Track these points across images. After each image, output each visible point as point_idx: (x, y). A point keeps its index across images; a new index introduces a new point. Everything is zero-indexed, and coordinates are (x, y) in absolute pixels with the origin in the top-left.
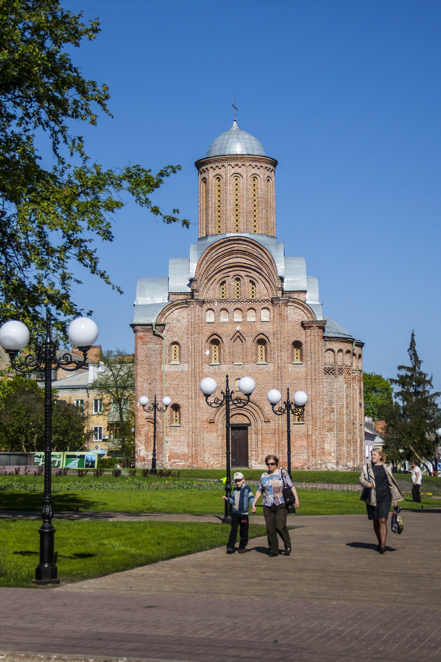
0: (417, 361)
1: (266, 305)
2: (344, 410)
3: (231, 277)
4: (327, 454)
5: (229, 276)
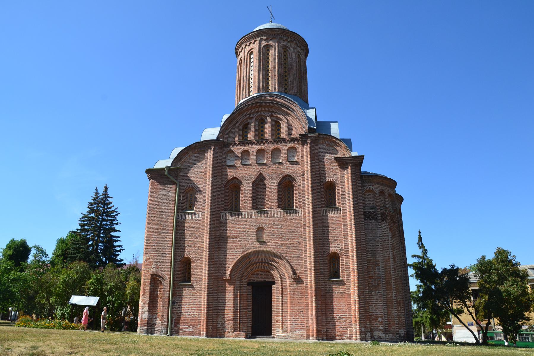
0: (425, 252)
1: (292, 144)
2: (391, 263)
3: (254, 119)
4: (373, 320)
5: (252, 118)
